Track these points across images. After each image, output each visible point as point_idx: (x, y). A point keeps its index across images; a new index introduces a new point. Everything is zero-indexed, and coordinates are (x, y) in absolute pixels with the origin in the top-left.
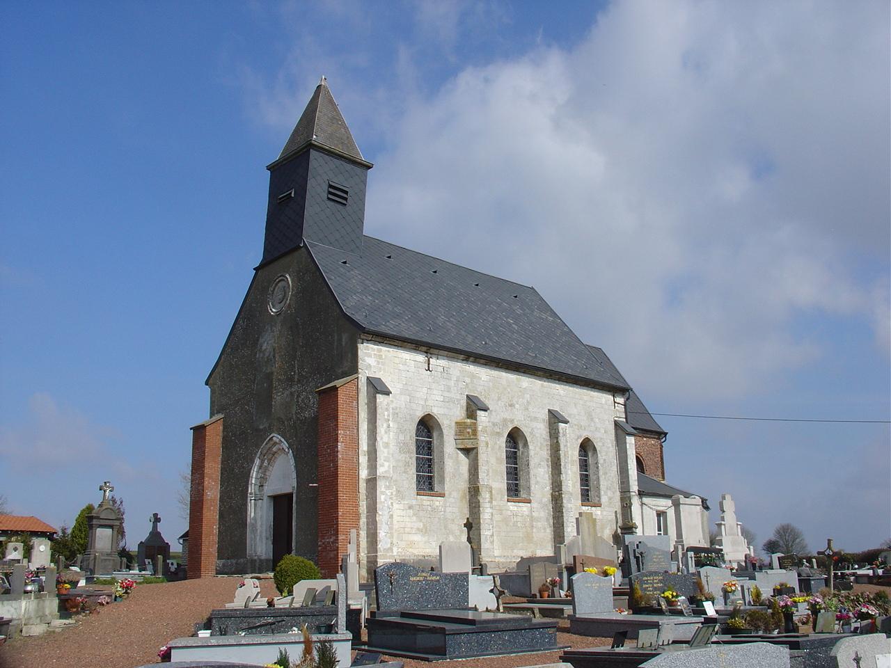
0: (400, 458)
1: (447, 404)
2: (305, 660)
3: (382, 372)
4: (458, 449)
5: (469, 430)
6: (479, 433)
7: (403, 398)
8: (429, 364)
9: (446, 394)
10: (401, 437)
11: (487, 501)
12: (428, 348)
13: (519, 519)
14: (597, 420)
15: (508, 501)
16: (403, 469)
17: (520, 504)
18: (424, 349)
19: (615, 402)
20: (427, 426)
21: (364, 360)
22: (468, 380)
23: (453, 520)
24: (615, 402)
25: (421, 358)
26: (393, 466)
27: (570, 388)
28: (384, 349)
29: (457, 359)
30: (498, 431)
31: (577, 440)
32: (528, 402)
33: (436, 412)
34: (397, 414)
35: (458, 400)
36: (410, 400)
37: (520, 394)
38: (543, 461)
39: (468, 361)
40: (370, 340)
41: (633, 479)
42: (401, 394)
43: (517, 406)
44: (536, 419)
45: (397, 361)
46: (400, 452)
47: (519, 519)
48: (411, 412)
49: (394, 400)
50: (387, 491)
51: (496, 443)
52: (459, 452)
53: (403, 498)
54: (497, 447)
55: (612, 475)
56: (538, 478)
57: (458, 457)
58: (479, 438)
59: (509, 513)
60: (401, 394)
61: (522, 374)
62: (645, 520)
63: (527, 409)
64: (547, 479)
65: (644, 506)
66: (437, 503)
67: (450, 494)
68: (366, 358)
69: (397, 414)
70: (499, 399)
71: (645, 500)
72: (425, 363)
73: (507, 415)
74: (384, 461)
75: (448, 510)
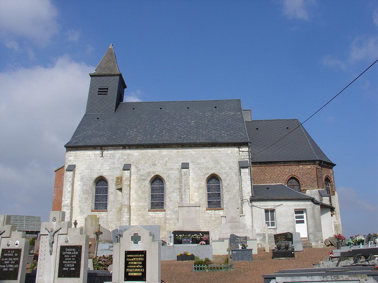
0: (83, 197)
1: (112, 170)
2: (105, 258)
3: (77, 162)
4: (117, 189)
5: (120, 180)
6: (123, 181)
7: (87, 171)
8: (102, 154)
9: (111, 166)
10: (85, 188)
11: (125, 212)
12: (102, 147)
13: (156, 219)
14: (223, 163)
15: (149, 211)
16: (84, 201)
17: (157, 212)
18: (99, 148)
19: (239, 151)
20: (157, 180)
21: (68, 159)
22: (125, 157)
23: (112, 222)
24: (239, 151)
25: (98, 152)
26: (79, 200)
27: (200, 150)
28: (78, 152)
29: (119, 149)
30: (144, 178)
31: (205, 176)
32: (166, 161)
33: (105, 174)
34: (83, 178)
35: (119, 167)
36: (91, 171)
37: (160, 158)
38: (176, 190)
39: (126, 149)
40: (72, 150)
41: (246, 192)
42: (86, 169)
43: (158, 165)
44: (172, 169)
45: (85, 156)
46: (83, 194)
47: (156, 219)
48: (91, 177)
49: (82, 172)
50: (67, 211)
51: (142, 184)
52: (118, 191)
53: (83, 214)
54: (143, 186)
55: (235, 191)
56: (171, 199)
57: (117, 193)
58: (123, 183)
59: (149, 217)
60: (86, 169)
61: (163, 148)
62: (254, 215)
63: (166, 165)
64: (179, 198)
65: (253, 207)
66: (103, 215)
67: (111, 210)
68: (69, 157)
69: (83, 178)
70: (146, 163)
71: (254, 203)
72: (100, 154)
73: (151, 170)
74: (68, 198)
75: (109, 217)
